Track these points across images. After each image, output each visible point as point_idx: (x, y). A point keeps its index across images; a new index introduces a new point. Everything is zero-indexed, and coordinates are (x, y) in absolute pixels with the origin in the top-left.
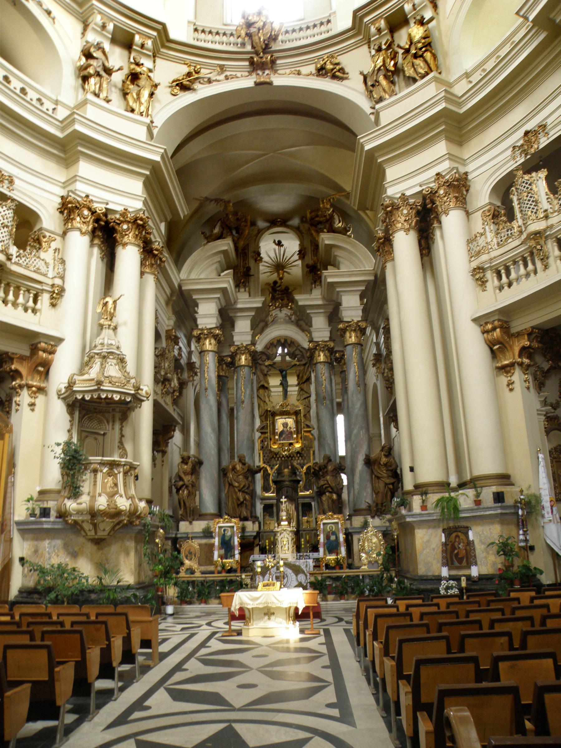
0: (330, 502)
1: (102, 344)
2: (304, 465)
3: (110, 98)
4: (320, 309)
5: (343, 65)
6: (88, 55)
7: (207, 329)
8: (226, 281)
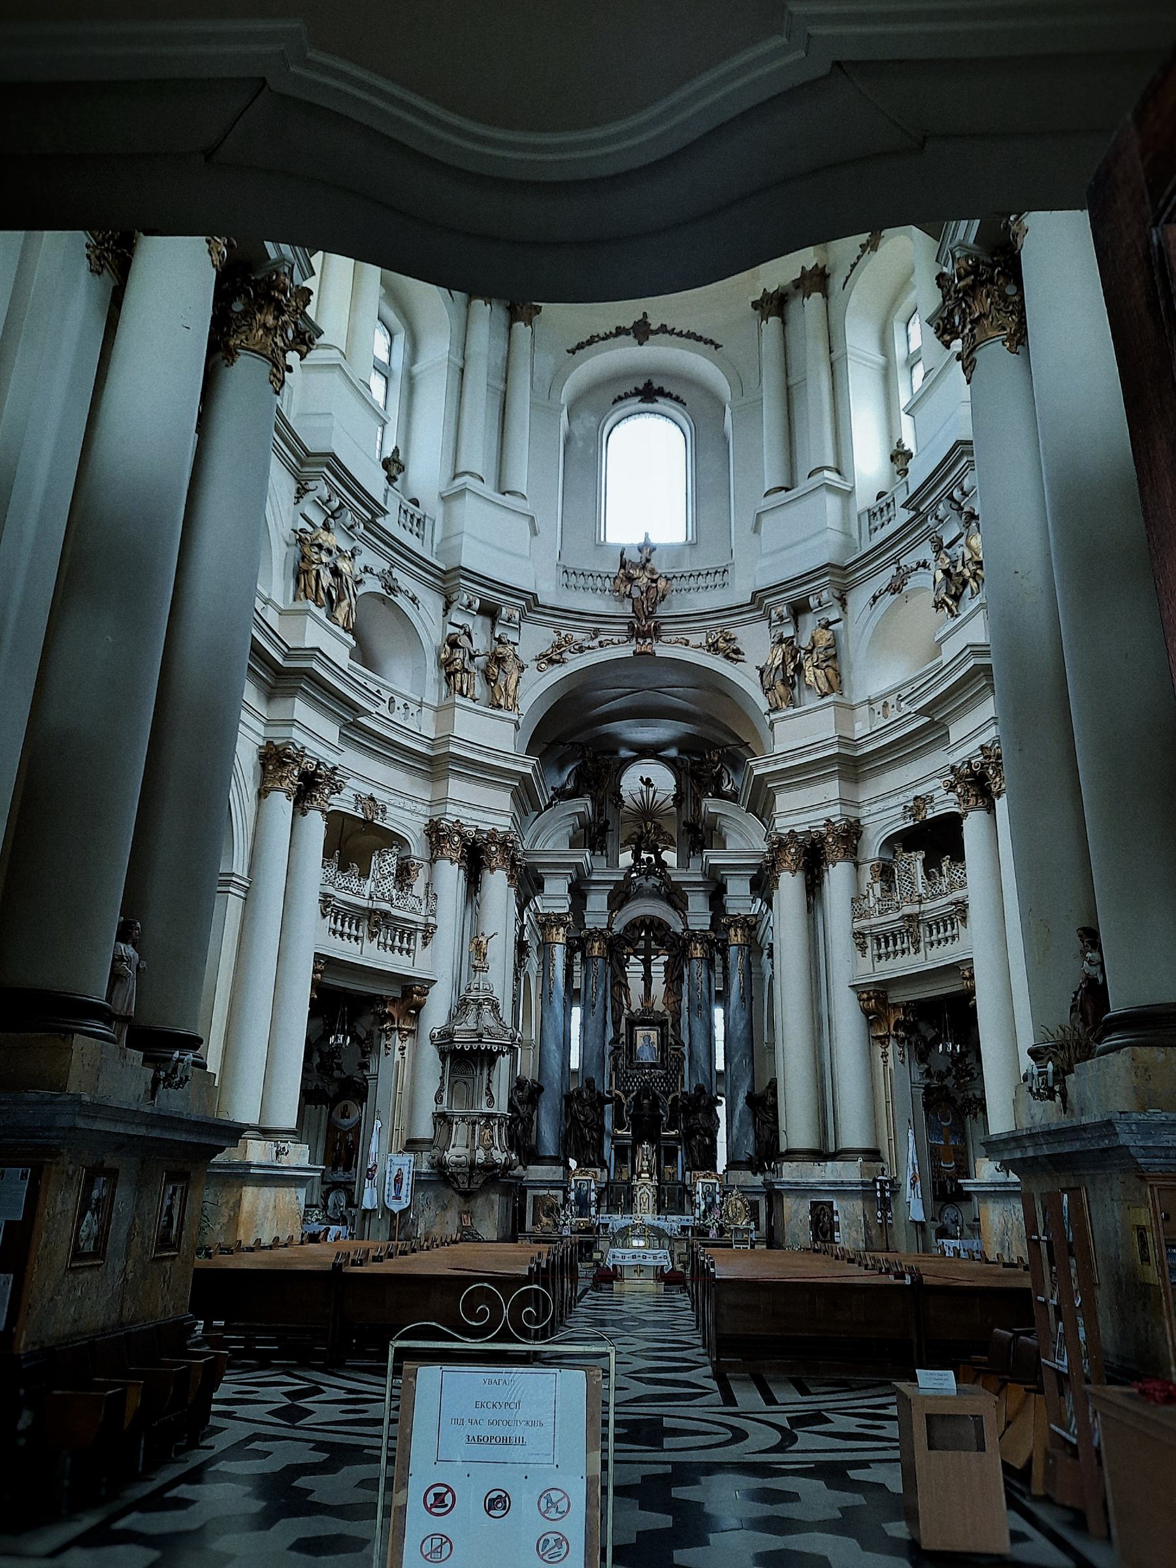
2: (669, 1093)
3: (477, 696)
5: (737, 645)
6: (454, 644)
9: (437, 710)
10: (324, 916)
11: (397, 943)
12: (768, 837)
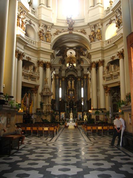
2: (74, 101)
8: (61, 65)
9: (38, 43)
10: (23, 76)
11: (34, 80)
12: (90, 62)
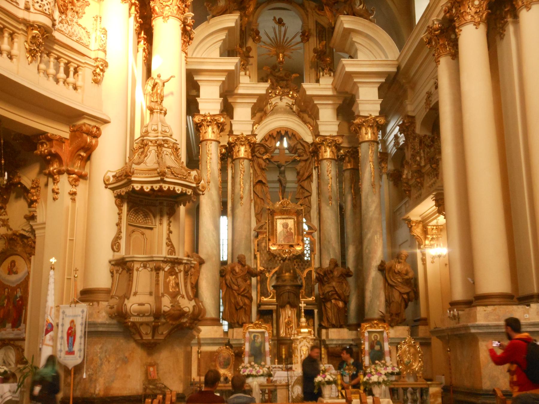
0: (336, 310)
1: (154, 130)
2: (304, 269)
4: (328, 100)
7: (210, 116)
11: (62, 75)
